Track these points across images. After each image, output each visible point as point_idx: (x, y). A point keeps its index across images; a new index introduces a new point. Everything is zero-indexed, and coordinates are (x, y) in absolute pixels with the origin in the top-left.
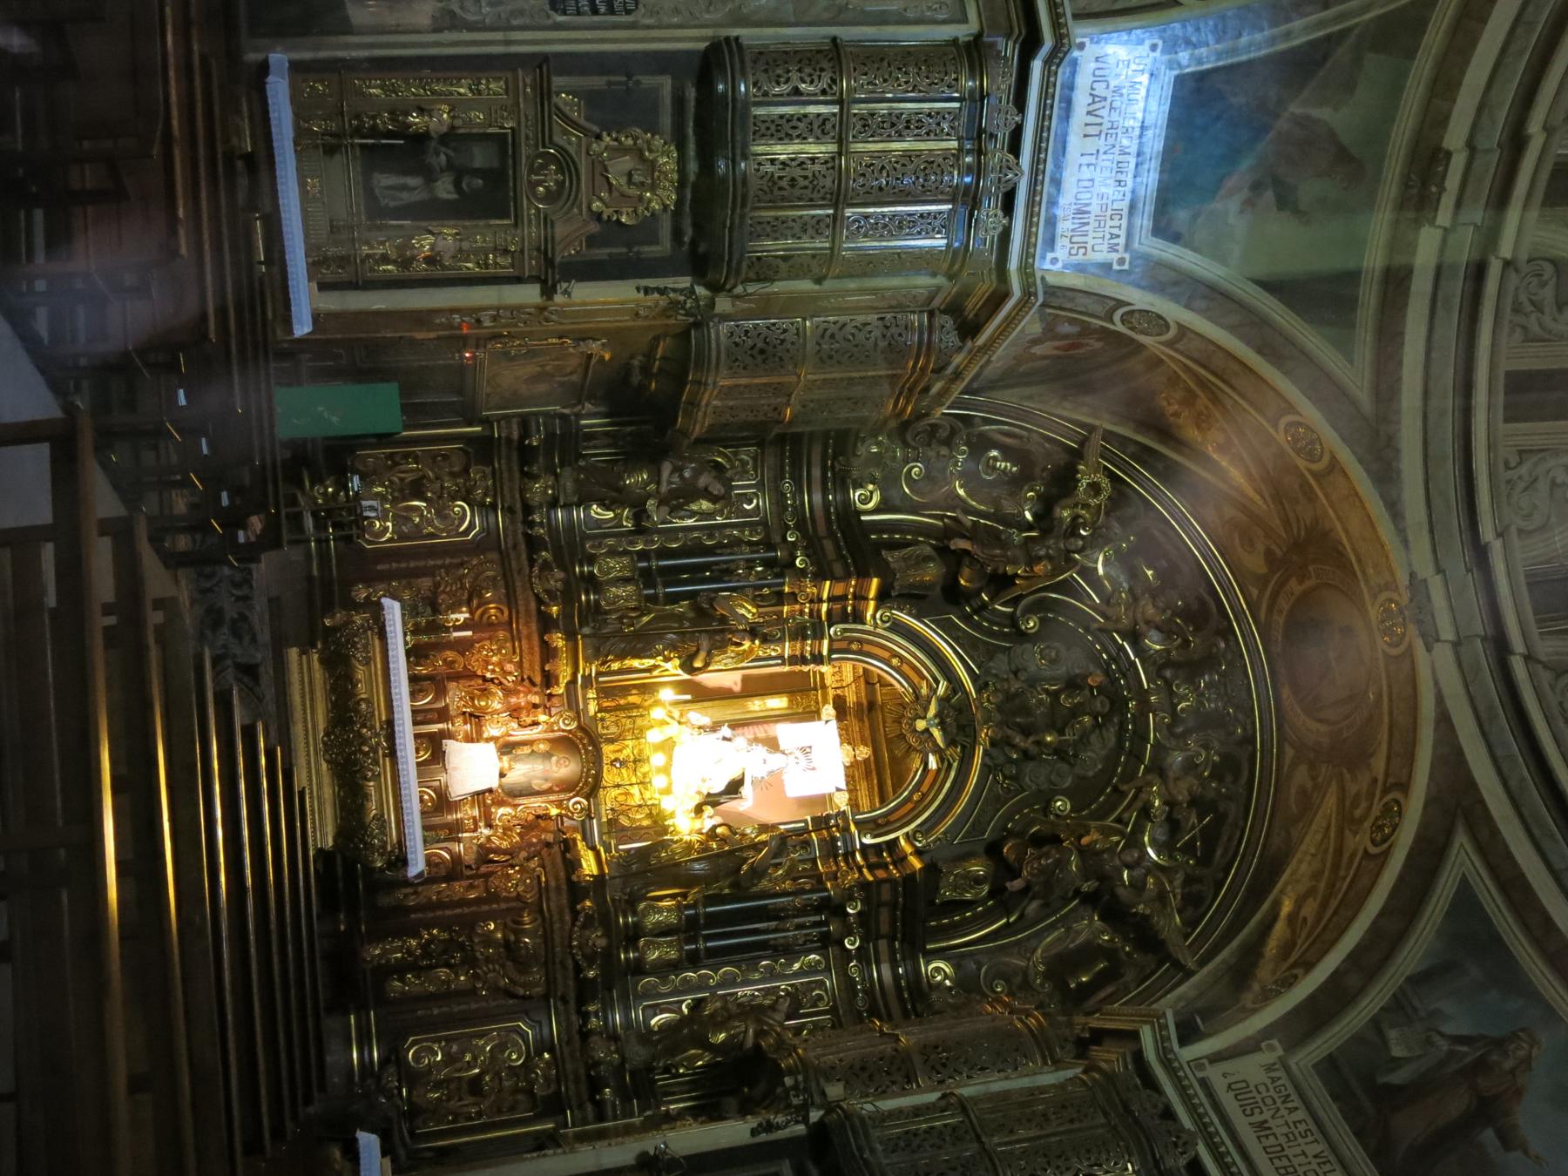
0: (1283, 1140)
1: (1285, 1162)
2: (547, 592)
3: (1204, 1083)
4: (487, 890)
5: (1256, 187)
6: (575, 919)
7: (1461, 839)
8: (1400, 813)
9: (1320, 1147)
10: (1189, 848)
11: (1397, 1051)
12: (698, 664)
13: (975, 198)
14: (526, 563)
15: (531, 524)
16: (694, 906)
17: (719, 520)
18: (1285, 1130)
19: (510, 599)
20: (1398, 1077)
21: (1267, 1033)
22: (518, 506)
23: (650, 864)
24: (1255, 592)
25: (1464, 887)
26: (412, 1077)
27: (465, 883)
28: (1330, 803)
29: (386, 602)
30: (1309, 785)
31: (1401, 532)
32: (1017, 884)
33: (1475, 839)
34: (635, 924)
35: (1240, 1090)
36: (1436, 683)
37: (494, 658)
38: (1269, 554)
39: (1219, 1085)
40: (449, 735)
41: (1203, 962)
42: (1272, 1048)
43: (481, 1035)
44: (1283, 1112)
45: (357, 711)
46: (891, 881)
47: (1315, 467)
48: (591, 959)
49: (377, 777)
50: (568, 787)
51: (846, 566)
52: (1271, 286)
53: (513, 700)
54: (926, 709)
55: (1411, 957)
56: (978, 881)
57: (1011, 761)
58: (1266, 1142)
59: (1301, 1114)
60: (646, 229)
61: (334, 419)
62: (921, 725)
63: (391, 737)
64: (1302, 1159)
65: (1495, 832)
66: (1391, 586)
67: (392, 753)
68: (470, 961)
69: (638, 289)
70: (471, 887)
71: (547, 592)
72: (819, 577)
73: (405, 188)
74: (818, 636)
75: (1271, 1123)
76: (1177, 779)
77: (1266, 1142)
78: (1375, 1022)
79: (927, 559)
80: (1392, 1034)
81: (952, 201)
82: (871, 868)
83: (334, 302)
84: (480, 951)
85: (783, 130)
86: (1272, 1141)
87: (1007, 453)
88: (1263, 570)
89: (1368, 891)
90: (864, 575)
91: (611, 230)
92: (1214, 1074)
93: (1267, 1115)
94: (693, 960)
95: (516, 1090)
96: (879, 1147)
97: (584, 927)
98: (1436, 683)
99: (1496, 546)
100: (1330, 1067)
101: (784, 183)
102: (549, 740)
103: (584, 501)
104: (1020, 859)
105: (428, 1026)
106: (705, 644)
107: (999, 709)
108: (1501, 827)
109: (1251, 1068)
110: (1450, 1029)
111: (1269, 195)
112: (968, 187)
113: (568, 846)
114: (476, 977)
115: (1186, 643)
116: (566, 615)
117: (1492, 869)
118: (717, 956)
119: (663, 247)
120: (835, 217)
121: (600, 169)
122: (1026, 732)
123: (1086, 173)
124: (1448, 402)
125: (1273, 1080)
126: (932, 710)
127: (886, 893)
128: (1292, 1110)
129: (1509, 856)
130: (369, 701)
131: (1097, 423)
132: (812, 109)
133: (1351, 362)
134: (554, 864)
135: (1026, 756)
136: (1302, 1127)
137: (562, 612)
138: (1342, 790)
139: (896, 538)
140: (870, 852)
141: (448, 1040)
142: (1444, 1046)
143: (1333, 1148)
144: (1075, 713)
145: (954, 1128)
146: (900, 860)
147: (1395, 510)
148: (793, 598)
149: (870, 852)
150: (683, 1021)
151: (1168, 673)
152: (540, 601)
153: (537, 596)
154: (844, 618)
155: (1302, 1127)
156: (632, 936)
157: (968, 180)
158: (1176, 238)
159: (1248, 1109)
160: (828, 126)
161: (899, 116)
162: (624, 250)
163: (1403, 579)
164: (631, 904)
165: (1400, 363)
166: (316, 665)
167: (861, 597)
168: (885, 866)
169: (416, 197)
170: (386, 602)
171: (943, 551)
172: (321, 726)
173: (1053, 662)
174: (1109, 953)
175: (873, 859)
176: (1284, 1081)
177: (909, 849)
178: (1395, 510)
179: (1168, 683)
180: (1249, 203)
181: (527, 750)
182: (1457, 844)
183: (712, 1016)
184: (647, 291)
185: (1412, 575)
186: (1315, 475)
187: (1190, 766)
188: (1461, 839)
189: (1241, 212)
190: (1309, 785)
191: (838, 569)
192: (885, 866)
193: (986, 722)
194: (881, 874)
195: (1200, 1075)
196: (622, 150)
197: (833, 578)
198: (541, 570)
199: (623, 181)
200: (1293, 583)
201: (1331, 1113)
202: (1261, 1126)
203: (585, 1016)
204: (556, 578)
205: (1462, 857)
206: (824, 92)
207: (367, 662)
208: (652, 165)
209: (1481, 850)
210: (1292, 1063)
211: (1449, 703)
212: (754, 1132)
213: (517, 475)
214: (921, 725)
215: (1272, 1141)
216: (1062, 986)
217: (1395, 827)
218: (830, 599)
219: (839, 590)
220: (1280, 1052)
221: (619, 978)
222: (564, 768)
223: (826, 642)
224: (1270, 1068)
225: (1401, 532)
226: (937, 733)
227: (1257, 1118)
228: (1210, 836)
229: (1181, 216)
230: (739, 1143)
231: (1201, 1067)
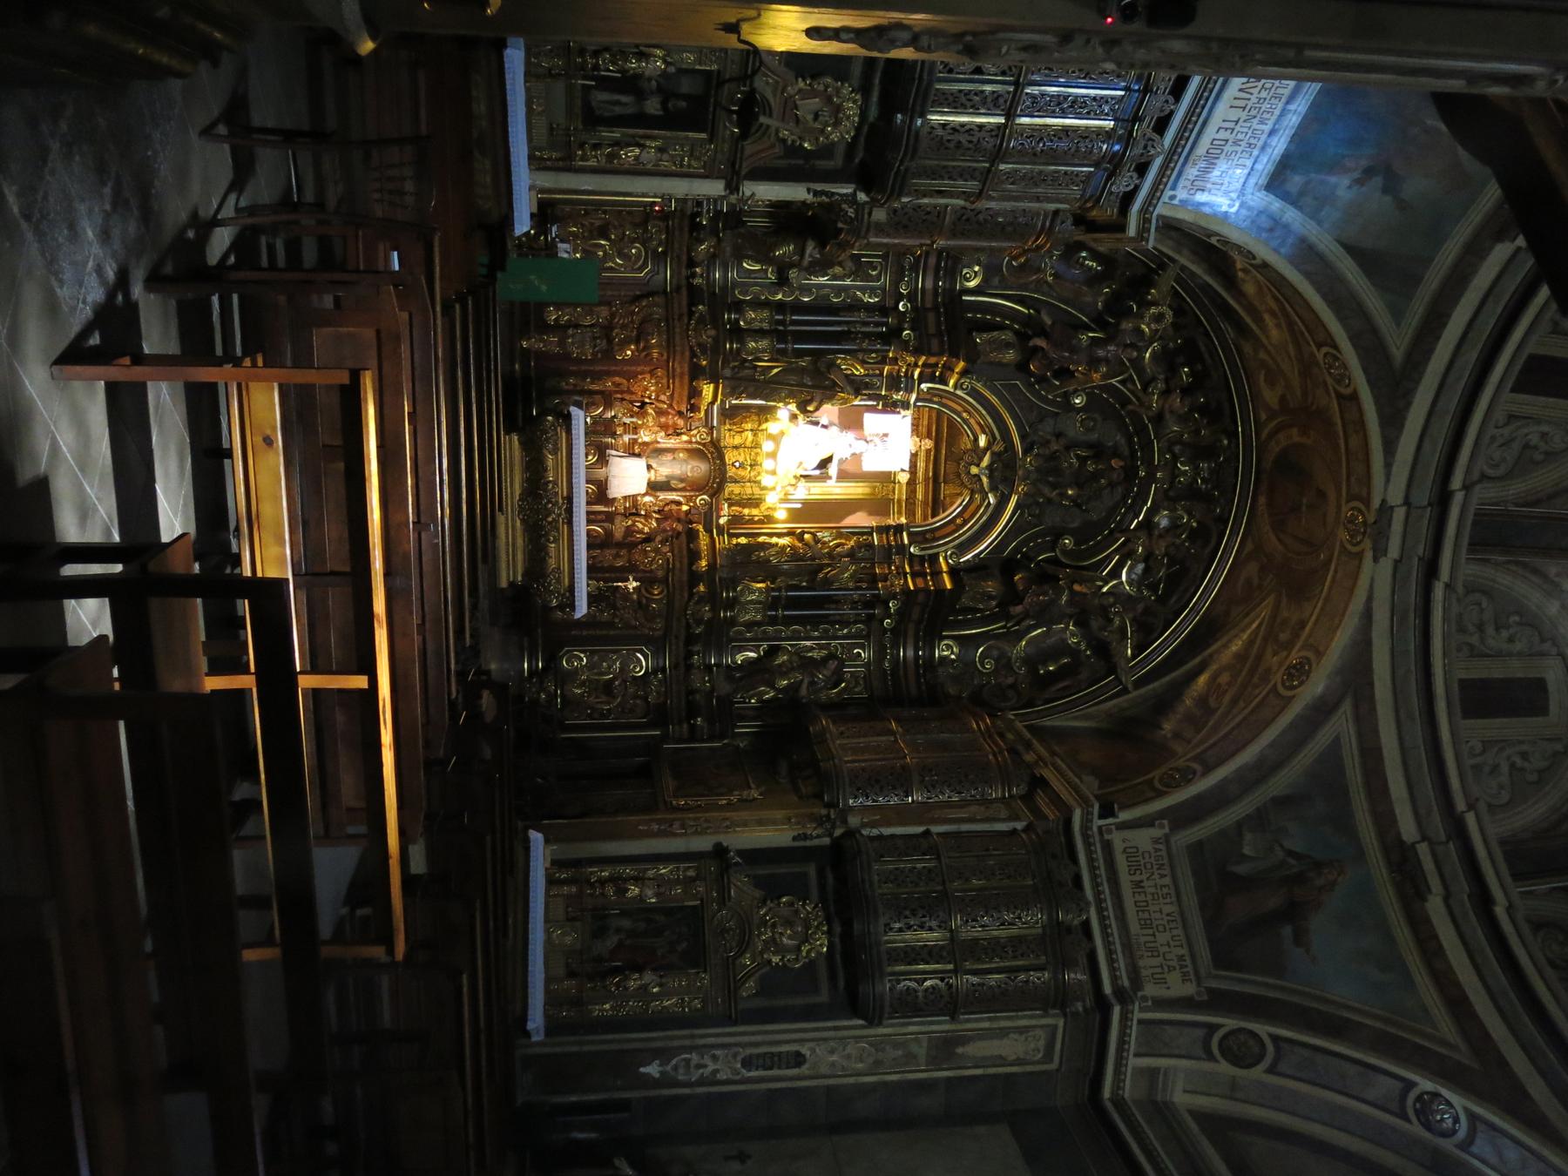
0: (1149, 897)
1: (1146, 915)
2: (699, 345)
3: (1108, 847)
4: (629, 561)
5: (1369, 172)
6: (691, 595)
7: (1347, 707)
8: (1309, 671)
9: (1173, 908)
10: (1153, 588)
11: (1247, 851)
12: (810, 408)
13: (1115, 168)
14: (685, 310)
15: (694, 275)
16: (779, 590)
17: (848, 282)
18: (1153, 890)
19: (669, 346)
20: (1241, 869)
21: (1162, 814)
22: (684, 258)
23: (750, 560)
24: (1263, 416)
25: (1337, 741)
26: (566, 678)
27: (614, 551)
28: (1265, 611)
29: (573, 409)
30: (1256, 581)
31: (1388, 465)
32: (1019, 609)
33: (1356, 707)
34: (735, 598)
35: (1131, 853)
36: (1371, 586)
37: (649, 387)
38: (1283, 399)
39: (1118, 846)
40: (612, 447)
41: (1139, 683)
42: (1162, 826)
43: (615, 652)
44: (1156, 876)
45: (546, 490)
46: (926, 590)
47: (1342, 390)
48: (699, 622)
49: (556, 541)
50: (697, 487)
51: (942, 343)
52: (1351, 250)
53: (663, 420)
54: (981, 459)
55: (1279, 784)
56: (991, 597)
57: (1038, 504)
58: (1138, 898)
59: (1167, 881)
60: (826, 151)
61: (544, 288)
62: (974, 470)
63: (570, 511)
64: (1158, 915)
65: (1373, 710)
66: (1367, 501)
67: (570, 523)
68: (614, 607)
69: (809, 190)
70: (617, 556)
71: (699, 345)
72: (917, 352)
73: (618, 103)
74: (909, 390)
75: (1145, 884)
76: (1160, 536)
77: (1138, 898)
78: (1239, 825)
79: (1008, 345)
80: (1248, 836)
81: (1096, 165)
82: (914, 575)
83: (547, 180)
84: (619, 603)
85: (958, 103)
86: (1142, 897)
87: (1095, 256)
88: (1276, 407)
89: (1268, 724)
90: (954, 354)
91: (794, 151)
92: (1117, 839)
93: (1144, 877)
94: (773, 621)
95: (636, 697)
96: (876, 878)
97: (698, 603)
98: (1371, 586)
99: (1459, 497)
100: (1197, 849)
101: (952, 145)
102: (687, 450)
103: (739, 257)
104: (1026, 590)
105: (580, 642)
106: (818, 398)
107: (1038, 470)
108: (1379, 707)
109: (1143, 839)
110: (1288, 844)
111: (1378, 181)
112: (1115, 154)
113: (692, 535)
114: (615, 615)
115: (1197, 432)
116: (713, 363)
117: (1360, 735)
118: (789, 621)
119: (837, 162)
120: (989, 170)
121: (789, 105)
122: (1054, 486)
123: (1223, 135)
124: (1417, 731)
125: (1157, 850)
126: (986, 461)
127: (921, 598)
128: (1162, 876)
129: (1376, 732)
130: (555, 483)
131: (1177, 257)
132: (988, 88)
133: (1398, 325)
134: (680, 551)
135: (1049, 501)
136: (1165, 890)
137: (710, 363)
138: (1274, 616)
139: (989, 321)
140: (916, 561)
141: (593, 652)
142: (1280, 854)
143: (1182, 914)
144: (1095, 476)
145: (930, 870)
146: (937, 573)
147: (1390, 448)
148: (895, 361)
149: (916, 561)
150: (759, 659)
151: (1177, 449)
152: (693, 355)
153: (691, 348)
154: (932, 379)
155: (1165, 890)
156: (731, 604)
157: (1117, 147)
158: (1285, 197)
159: (1134, 868)
160: (1001, 101)
161: (1066, 98)
162: (801, 162)
163: (1376, 503)
164: (732, 583)
165: (1438, 338)
166: (516, 443)
167: (949, 368)
168: (924, 575)
169: (630, 111)
170: (573, 409)
171: (1023, 337)
172: (518, 492)
173: (1089, 430)
174: (1074, 652)
175: (917, 568)
176: (1164, 853)
177: (945, 568)
178: (1390, 448)
179: (1175, 458)
180: (1359, 182)
181: (669, 457)
182: (1341, 711)
183: (780, 666)
184: (816, 193)
185: (1384, 501)
186: (1336, 392)
187: (1175, 526)
188: (1347, 707)
189: (1349, 187)
190: (1256, 581)
191: (935, 343)
192: (924, 575)
193: (1024, 479)
194: (920, 581)
195: (1107, 837)
196: (813, 94)
197: (930, 354)
198: (697, 323)
199: (810, 117)
200: (1295, 431)
201: (1188, 884)
202: (1138, 884)
203: (689, 655)
204: (707, 336)
205: (1342, 724)
206: (1003, 73)
207: (555, 451)
208: (838, 109)
209: (1358, 719)
210: (1173, 839)
211: (1375, 605)
212: (794, 839)
213: (686, 235)
214: (974, 470)
215: (1142, 897)
216: (1033, 670)
217: (1301, 683)
218: (924, 365)
219: (933, 360)
220: (1167, 830)
221: (720, 635)
222: (697, 469)
223: (914, 396)
224: (1156, 841)
225: (1388, 465)
226: (985, 480)
227: (1137, 878)
228: (1173, 581)
229: (1296, 181)
230: (783, 845)
231: (1110, 832)
